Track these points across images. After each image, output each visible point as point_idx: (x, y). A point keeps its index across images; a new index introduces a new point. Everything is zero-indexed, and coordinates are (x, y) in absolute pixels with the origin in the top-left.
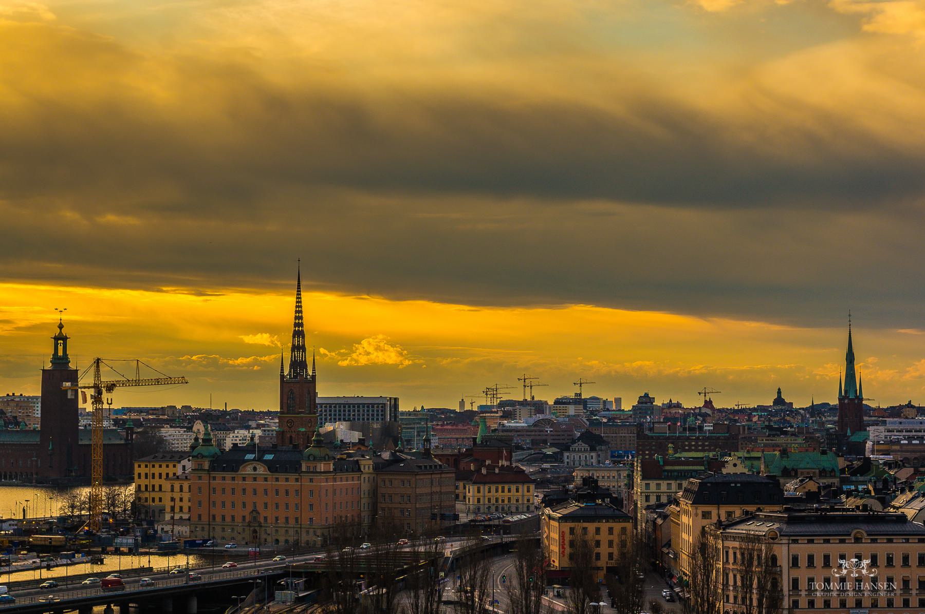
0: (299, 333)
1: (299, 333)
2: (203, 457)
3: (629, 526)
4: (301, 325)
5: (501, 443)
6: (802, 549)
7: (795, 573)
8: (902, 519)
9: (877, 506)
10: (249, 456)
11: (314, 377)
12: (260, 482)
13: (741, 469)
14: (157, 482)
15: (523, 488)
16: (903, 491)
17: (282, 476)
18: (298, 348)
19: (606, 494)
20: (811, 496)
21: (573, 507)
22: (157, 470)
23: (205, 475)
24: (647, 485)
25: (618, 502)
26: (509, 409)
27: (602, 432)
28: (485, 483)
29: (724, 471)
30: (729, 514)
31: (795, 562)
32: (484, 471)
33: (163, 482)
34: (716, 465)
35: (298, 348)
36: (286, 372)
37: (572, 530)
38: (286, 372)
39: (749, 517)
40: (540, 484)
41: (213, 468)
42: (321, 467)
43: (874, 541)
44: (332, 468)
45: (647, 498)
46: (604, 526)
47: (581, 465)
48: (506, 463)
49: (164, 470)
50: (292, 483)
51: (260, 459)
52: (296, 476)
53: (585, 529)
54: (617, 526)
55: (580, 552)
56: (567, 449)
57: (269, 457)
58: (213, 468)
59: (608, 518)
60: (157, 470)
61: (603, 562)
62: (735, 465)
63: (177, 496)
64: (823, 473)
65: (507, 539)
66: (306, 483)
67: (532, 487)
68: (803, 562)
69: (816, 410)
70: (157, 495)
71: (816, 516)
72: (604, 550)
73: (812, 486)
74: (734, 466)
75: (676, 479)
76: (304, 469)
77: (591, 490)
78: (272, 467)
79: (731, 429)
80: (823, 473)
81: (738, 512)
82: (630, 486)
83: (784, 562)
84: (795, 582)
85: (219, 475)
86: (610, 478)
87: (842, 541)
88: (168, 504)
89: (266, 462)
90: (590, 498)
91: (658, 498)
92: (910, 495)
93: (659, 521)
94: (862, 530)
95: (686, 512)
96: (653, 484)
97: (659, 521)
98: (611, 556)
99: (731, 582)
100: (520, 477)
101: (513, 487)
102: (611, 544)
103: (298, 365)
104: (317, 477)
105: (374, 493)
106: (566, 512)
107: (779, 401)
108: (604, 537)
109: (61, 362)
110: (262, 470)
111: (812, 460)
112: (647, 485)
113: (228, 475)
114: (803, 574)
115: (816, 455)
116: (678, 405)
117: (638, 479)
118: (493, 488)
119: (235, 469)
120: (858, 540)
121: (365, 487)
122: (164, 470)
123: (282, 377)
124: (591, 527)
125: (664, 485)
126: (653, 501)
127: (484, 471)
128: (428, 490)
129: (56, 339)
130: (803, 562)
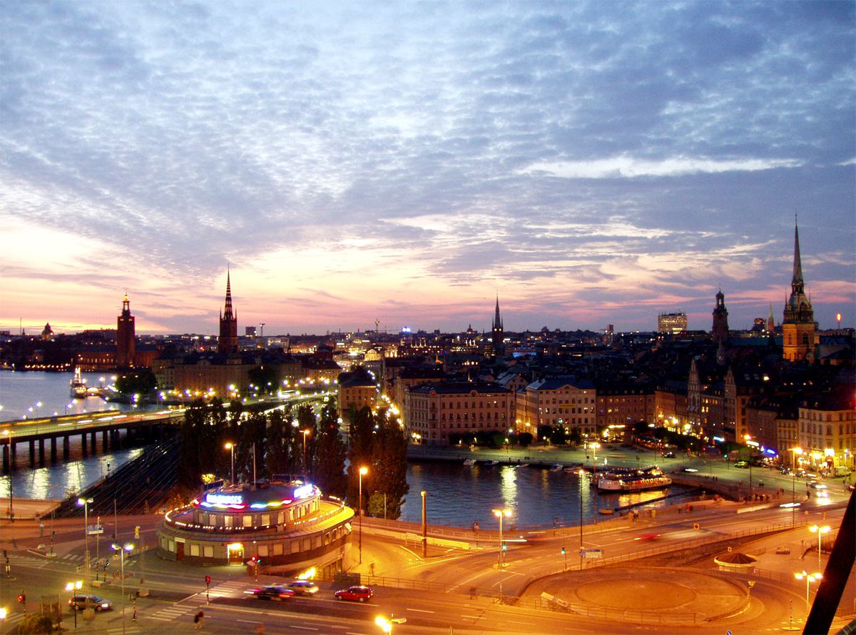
0: (229, 298)
1: (229, 298)
2: (180, 358)
4: (230, 295)
11: (236, 319)
16: (502, 372)
18: (229, 306)
24: (388, 370)
29: (424, 362)
31: (444, 406)
32: (318, 363)
35: (229, 306)
36: (223, 317)
38: (223, 317)
42: (236, 362)
44: (182, 362)
51: (206, 358)
52: (224, 366)
53: (348, 391)
57: (211, 357)
62: (429, 360)
68: (447, 406)
76: (228, 363)
83: (438, 406)
84: (444, 418)
89: (210, 360)
92: (505, 373)
99: (414, 416)
103: (229, 313)
107: (470, 330)
109: (126, 313)
110: (208, 363)
112: (388, 370)
114: (447, 412)
119: (195, 363)
120: (474, 395)
123: (221, 319)
127: (318, 363)
129: (124, 302)
130: (447, 406)
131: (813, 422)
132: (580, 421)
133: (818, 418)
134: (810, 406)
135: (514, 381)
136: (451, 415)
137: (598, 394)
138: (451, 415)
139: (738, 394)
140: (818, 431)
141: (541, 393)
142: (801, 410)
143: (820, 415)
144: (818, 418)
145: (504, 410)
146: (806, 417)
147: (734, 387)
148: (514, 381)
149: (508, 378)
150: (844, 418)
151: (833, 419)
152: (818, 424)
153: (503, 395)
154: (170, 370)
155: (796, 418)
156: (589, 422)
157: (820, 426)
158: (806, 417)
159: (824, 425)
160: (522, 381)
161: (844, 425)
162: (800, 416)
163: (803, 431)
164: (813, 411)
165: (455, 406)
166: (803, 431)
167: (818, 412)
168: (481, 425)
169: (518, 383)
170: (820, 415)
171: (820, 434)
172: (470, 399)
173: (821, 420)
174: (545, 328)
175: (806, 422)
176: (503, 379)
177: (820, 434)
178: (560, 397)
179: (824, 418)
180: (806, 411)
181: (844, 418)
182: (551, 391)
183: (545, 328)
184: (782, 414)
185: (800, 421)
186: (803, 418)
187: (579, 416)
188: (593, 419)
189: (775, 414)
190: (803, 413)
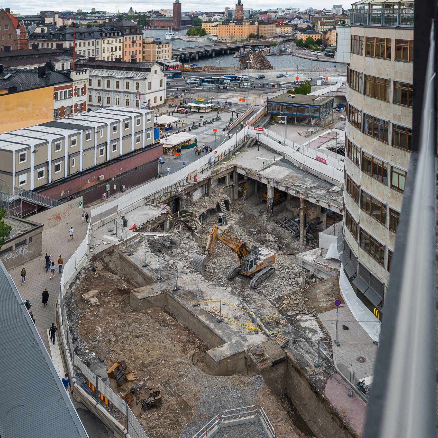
10: (231, 22)
12: (233, 27)
14: (207, 28)
17: (238, 26)
22: (207, 25)
23: (221, 26)
33: (210, 27)
41: (223, 24)
42: (247, 24)
49: (210, 25)
50: (241, 27)
51: (233, 22)
58: (223, 24)
60: (207, 25)
63: (215, 30)
66: (243, 27)
70: (209, 30)
78: (236, 24)
85: (224, 26)
88: (211, 32)
104: (246, 26)
105: (258, 29)
110: (234, 24)
113: (226, 26)
121: (256, 28)
122: (210, 25)
154: (213, 28)
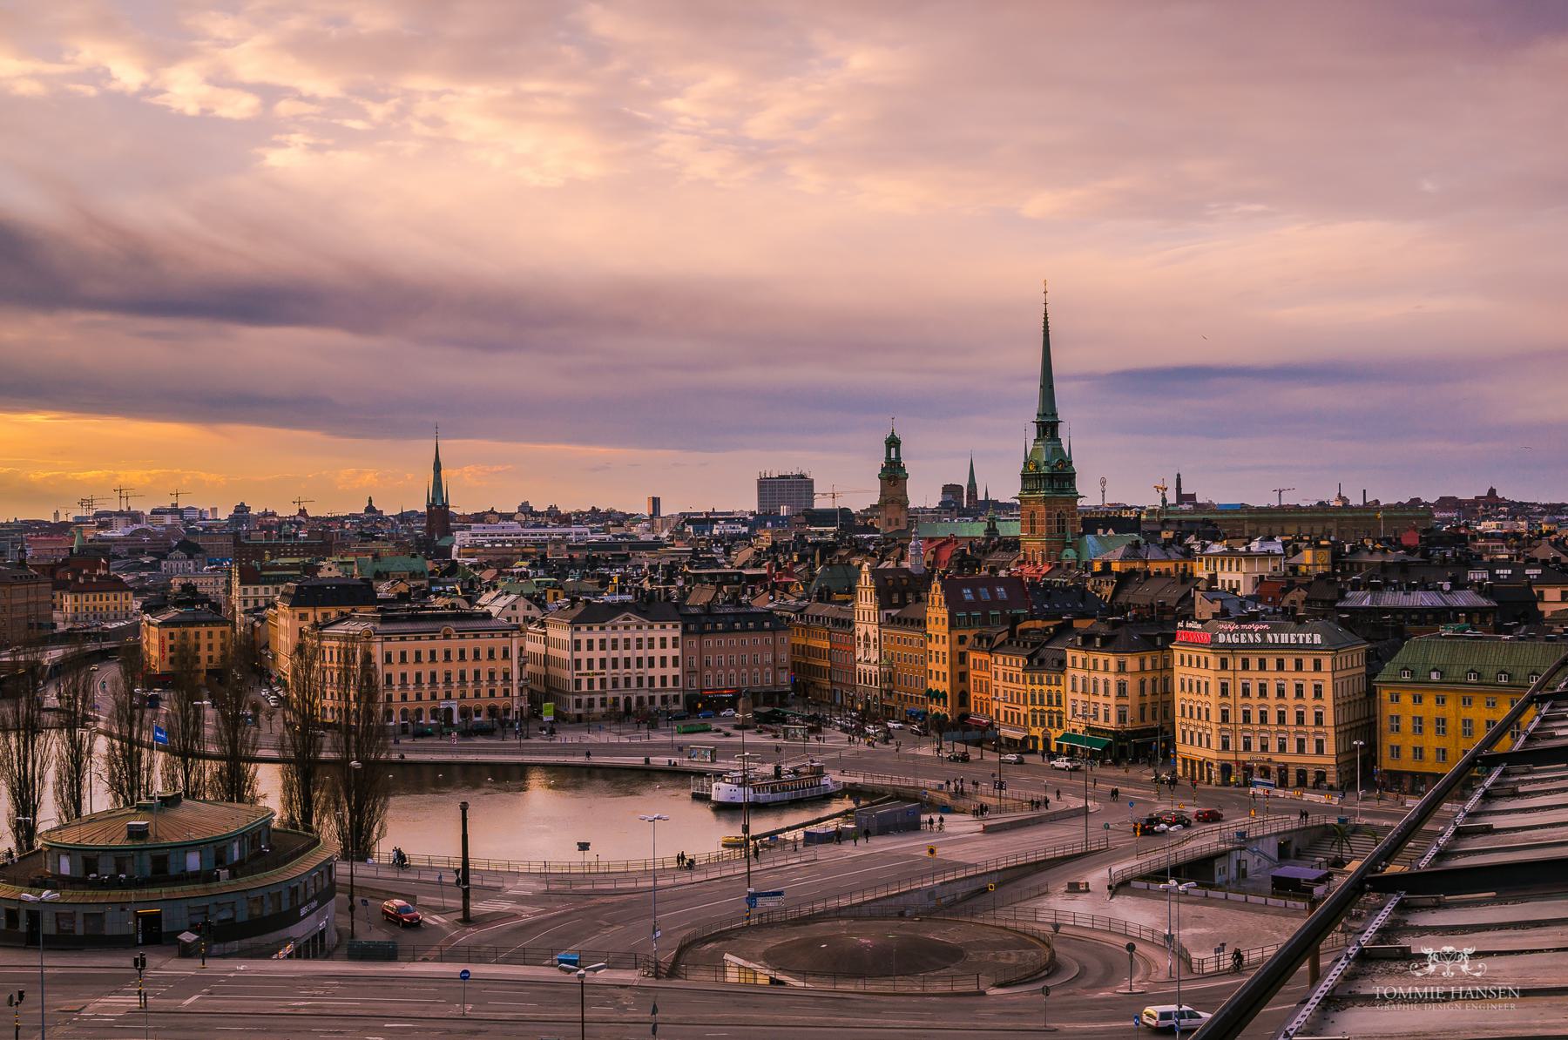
3: (228, 629)
5: (97, 553)
6: (395, 647)
7: (388, 669)
8: (488, 616)
9: (464, 605)
13: (335, 573)
15: (121, 596)
16: (488, 590)
19: (205, 599)
20: (403, 597)
21: (173, 613)
24: (245, 591)
25: (216, 607)
26: (105, 520)
27: (199, 541)
28: (82, 592)
30: (325, 615)
32: (81, 580)
34: (312, 569)
37: (172, 635)
39: (344, 618)
40: (138, 592)
43: (462, 637)
45: (245, 603)
46: (203, 630)
47: (179, 573)
48: (103, 572)
54: (217, 630)
55: (183, 656)
56: (165, 557)
59: (207, 622)
61: (203, 664)
64: (413, 576)
65: (106, 645)
67: (131, 595)
68: (396, 658)
69: (404, 517)
71: (406, 613)
72: (203, 653)
73: (403, 588)
74: (329, 570)
75: (273, 583)
77: (190, 595)
79: (325, 536)
80: (413, 576)
81: (333, 613)
82: (228, 591)
83: (378, 660)
84: (389, 677)
86: (208, 584)
87: (433, 638)
90: (190, 603)
91: (256, 602)
92: (494, 594)
93: (258, 624)
94: (452, 626)
95: (284, 615)
96: (251, 589)
97: (258, 624)
98: (210, 658)
100: (117, 586)
101: (111, 596)
102: (210, 647)
106: (166, 617)
107: (370, 509)
108: (204, 641)
111: (402, 564)
112: (245, 591)
114: (396, 670)
115: (406, 559)
116: (273, 514)
117: (236, 584)
118: (91, 597)
120: (447, 637)
124: (192, 630)
125: (261, 589)
126: (251, 605)
128: (24, 600)
130: (396, 658)
131: (1093, 675)
132: (652, 679)
133: (1101, 666)
134: (1088, 642)
135: (514, 608)
136: (433, 675)
137: (685, 632)
138: (419, 675)
139: (952, 626)
140: (1101, 690)
141: (578, 629)
142: (1070, 654)
143: (1106, 662)
144: (1101, 666)
145: (506, 664)
146: (1079, 664)
147: (943, 613)
148: (514, 608)
149: (502, 602)
150: (1148, 665)
151: (1128, 669)
152: (1101, 677)
153: (505, 636)
155: (1062, 664)
156: (670, 685)
157: (1106, 682)
158: (1079, 664)
159: (1112, 678)
160: (529, 608)
161: (1148, 678)
162: (1069, 663)
163: (1074, 690)
164: (1092, 656)
165: (469, 655)
166: (1074, 690)
167: (1101, 658)
168: (463, 696)
169: (522, 611)
170: (1106, 662)
171: (1106, 694)
172: (440, 645)
173: (1106, 669)
174: (525, 505)
175: (1080, 674)
176: (493, 604)
177: (1106, 694)
178: (621, 635)
179: (1113, 666)
180: (1080, 655)
181: (1148, 665)
182: (596, 628)
183: (525, 505)
184: (1036, 662)
185: (1070, 672)
186: (1074, 665)
187: (651, 672)
188: (675, 678)
189: (1022, 661)
190: (1074, 658)
